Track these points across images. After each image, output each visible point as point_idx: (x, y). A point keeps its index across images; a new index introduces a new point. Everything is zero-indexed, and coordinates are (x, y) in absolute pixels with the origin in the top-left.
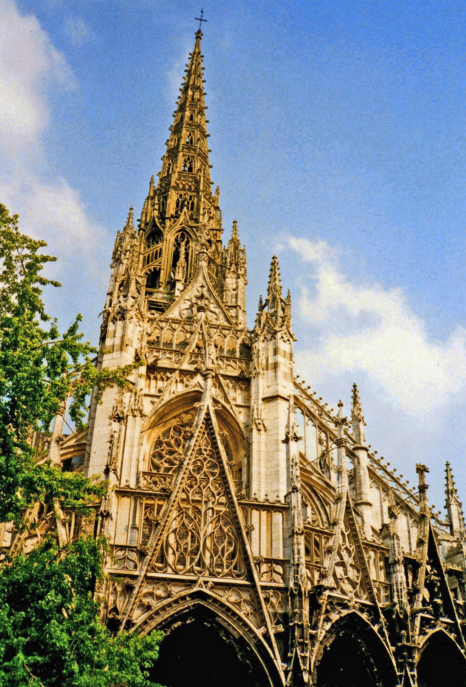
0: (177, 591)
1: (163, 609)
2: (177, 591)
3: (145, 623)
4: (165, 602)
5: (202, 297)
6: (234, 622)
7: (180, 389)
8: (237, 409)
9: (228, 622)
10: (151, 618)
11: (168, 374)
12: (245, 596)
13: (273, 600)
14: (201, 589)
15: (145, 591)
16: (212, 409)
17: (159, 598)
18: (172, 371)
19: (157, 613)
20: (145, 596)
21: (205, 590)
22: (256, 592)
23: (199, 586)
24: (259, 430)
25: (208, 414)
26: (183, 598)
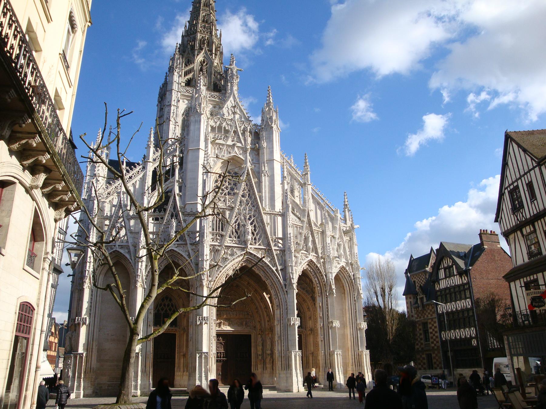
18: (223, 145)
22: (272, 251)
25: (248, 170)
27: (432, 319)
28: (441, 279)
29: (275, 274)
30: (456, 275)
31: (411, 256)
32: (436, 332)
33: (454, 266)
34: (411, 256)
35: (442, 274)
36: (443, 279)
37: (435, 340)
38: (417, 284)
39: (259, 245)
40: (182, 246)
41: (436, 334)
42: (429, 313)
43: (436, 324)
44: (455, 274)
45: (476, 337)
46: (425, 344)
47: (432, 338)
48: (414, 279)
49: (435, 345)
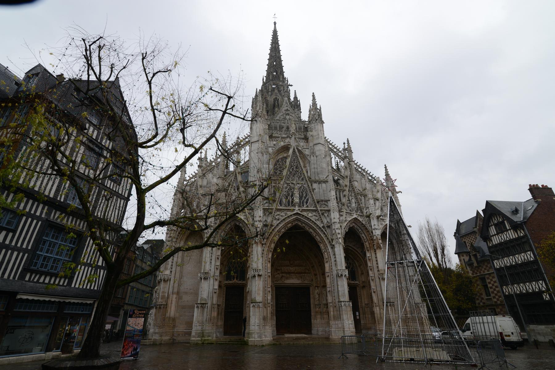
0: (289, 213)
1: (284, 220)
2: (288, 213)
3: (278, 225)
4: (284, 218)
5: (287, 110)
7: (282, 144)
12: (314, 214)
13: (326, 215)
15: (276, 214)
16: (295, 147)
17: (282, 216)
19: (282, 221)
26: (291, 215)
27: (489, 274)
28: (493, 236)
29: (322, 231)
30: (510, 230)
31: (458, 221)
32: (497, 287)
33: (505, 222)
34: (458, 221)
35: (493, 230)
36: (495, 235)
37: (496, 295)
38: (467, 244)
39: (307, 207)
41: (497, 289)
42: (485, 269)
43: (496, 279)
44: (508, 228)
45: (548, 290)
46: (487, 299)
47: (493, 292)
48: (464, 240)
49: (498, 300)
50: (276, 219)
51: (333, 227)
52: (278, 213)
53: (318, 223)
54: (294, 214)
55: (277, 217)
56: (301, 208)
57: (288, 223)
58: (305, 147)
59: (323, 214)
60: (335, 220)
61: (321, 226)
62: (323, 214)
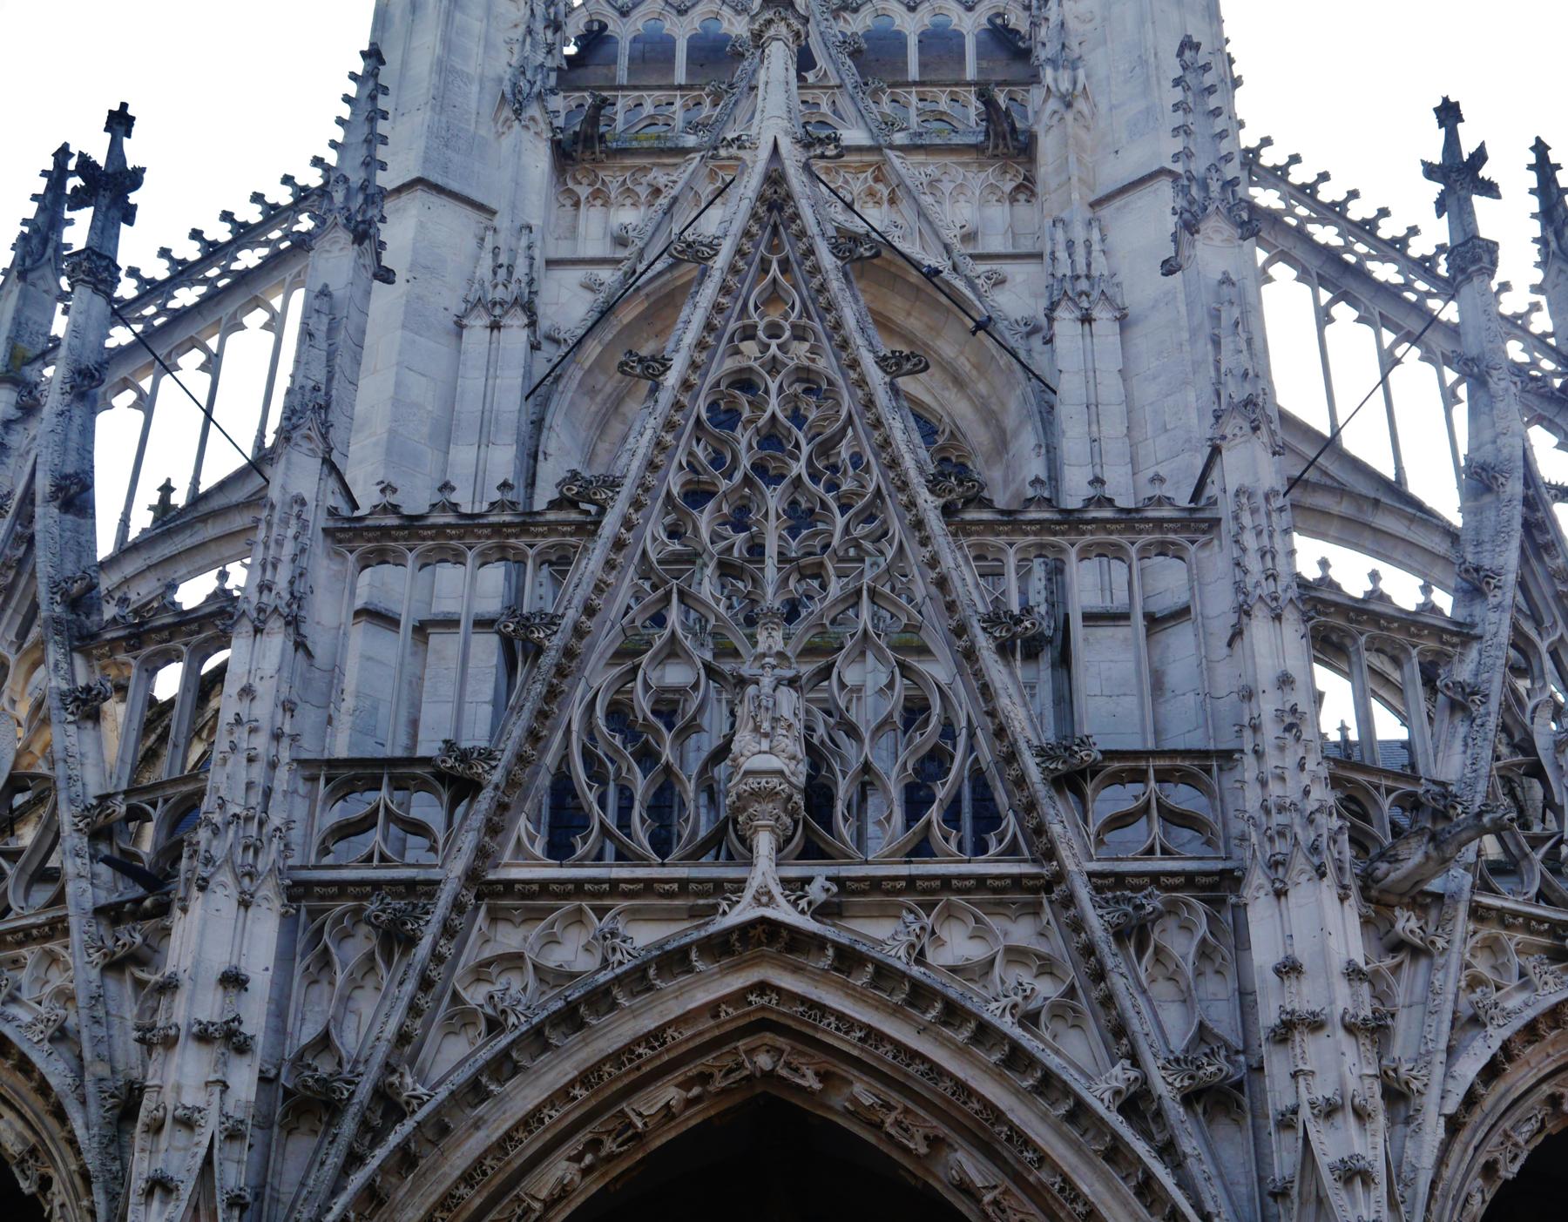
0: (645, 936)
1: (570, 1019)
3: (474, 1092)
6: (960, 1051)
8: (982, 268)
9: (924, 1059)
10: (503, 1067)
11: (659, 177)
12: (1021, 932)
14: (769, 913)
15: (472, 953)
16: (792, 156)
19: (537, 1040)
20: (481, 971)
21: (784, 913)
22: (1069, 901)
23: (757, 900)
24: (1087, 319)
25: (775, 178)
26: (674, 961)
29: (1116, 1153)
40: (29, 953)
50: (462, 1017)
51: (1278, 1092)
52: (509, 938)
53: (1074, 1053)
54: (723, 947)
55: (475, 996)
56: (820, 872)
57: (636, 1067)
58: (995, 244)
59: (1134, 934)
60: (1305, 997)
61: (1101, 1086)
62: (1134, 934)
